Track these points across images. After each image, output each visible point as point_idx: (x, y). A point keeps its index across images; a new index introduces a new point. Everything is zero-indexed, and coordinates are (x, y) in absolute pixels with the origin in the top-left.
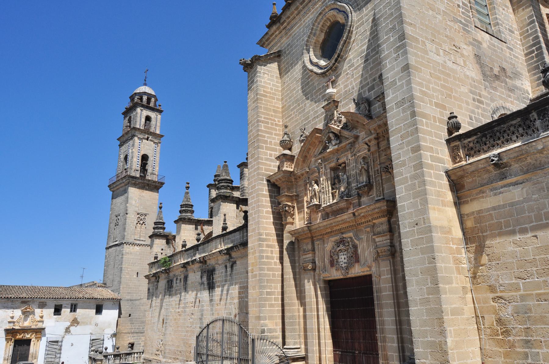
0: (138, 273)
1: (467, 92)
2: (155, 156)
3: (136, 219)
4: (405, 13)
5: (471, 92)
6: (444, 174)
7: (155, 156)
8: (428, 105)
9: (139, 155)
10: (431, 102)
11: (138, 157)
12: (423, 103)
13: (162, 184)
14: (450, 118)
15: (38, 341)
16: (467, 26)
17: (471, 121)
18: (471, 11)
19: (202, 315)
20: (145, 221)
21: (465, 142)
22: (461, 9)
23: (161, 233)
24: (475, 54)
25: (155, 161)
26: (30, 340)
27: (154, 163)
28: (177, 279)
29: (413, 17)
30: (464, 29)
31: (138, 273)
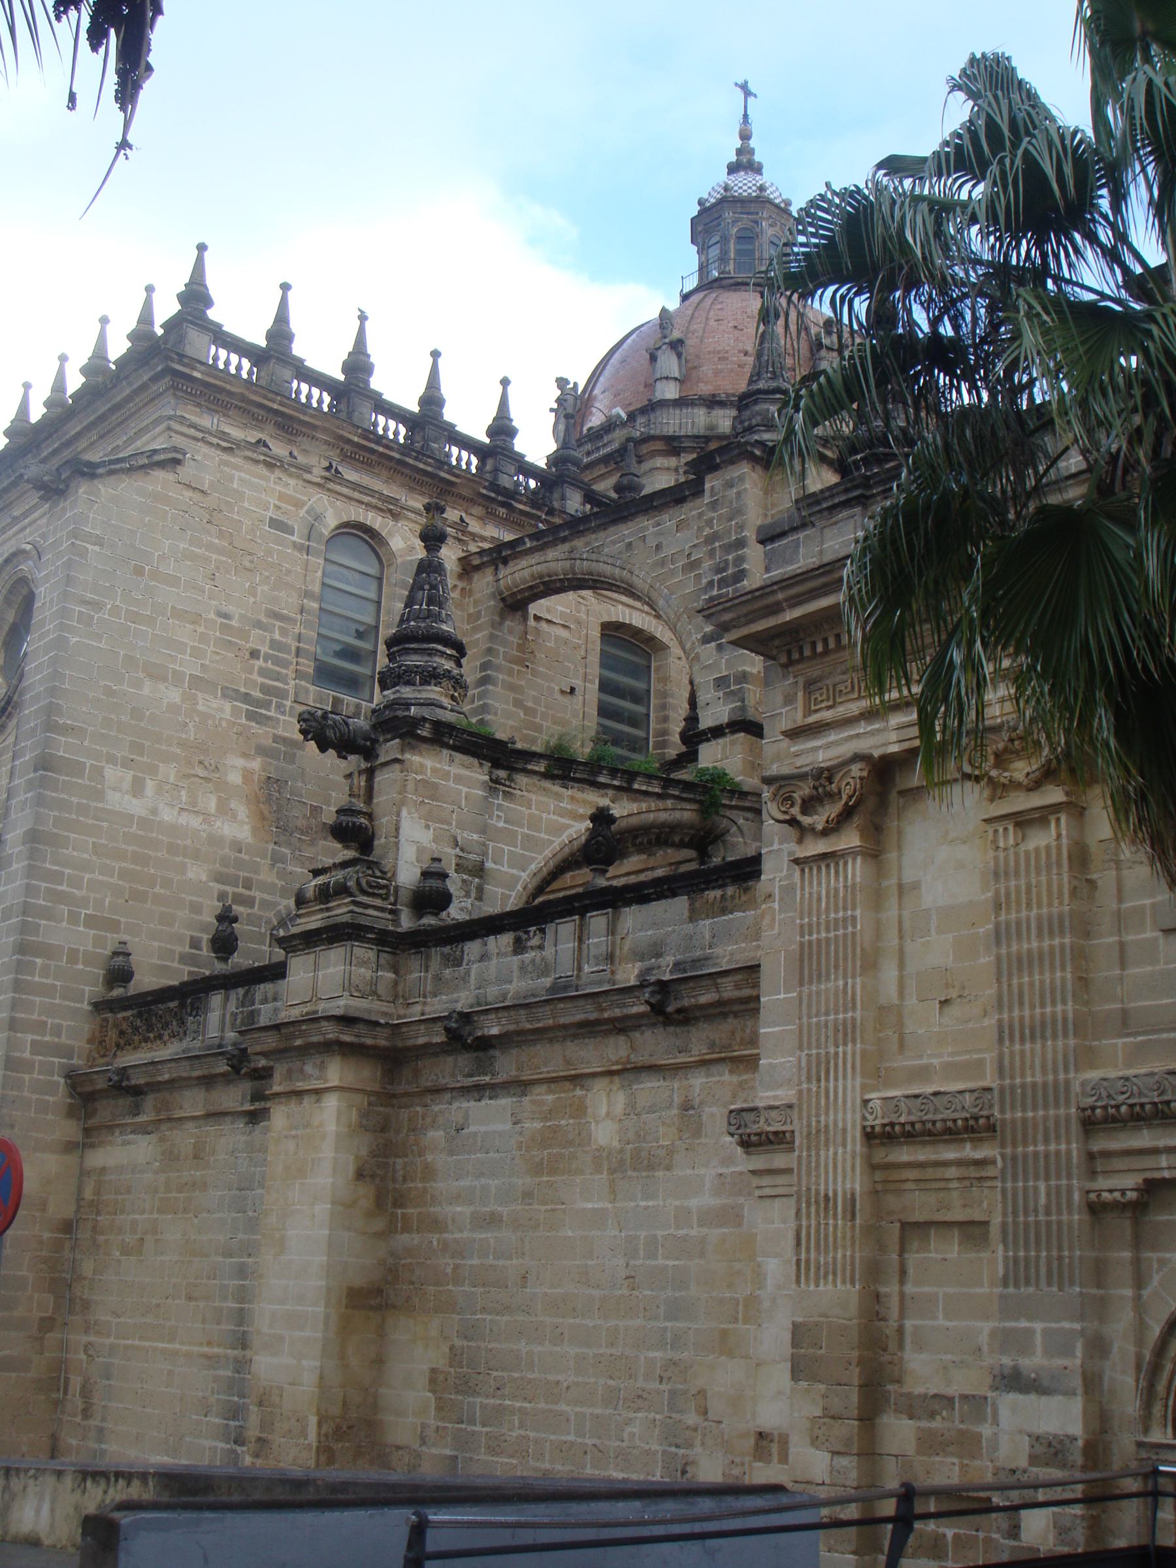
1: (204, 878)
4: (60, 702)
5: (219, 878)
6: (62, 1081)
8: (64, 924)
10: (73, 918)
12: (49, 920)
14: (116, 954)
16: (267, 705)
17: (194, 951)
18: (294, 660)
21: (120, 1015)
22: (260, 663)
24: (269, 778)
29: (84, 709)
30: (251, 716)
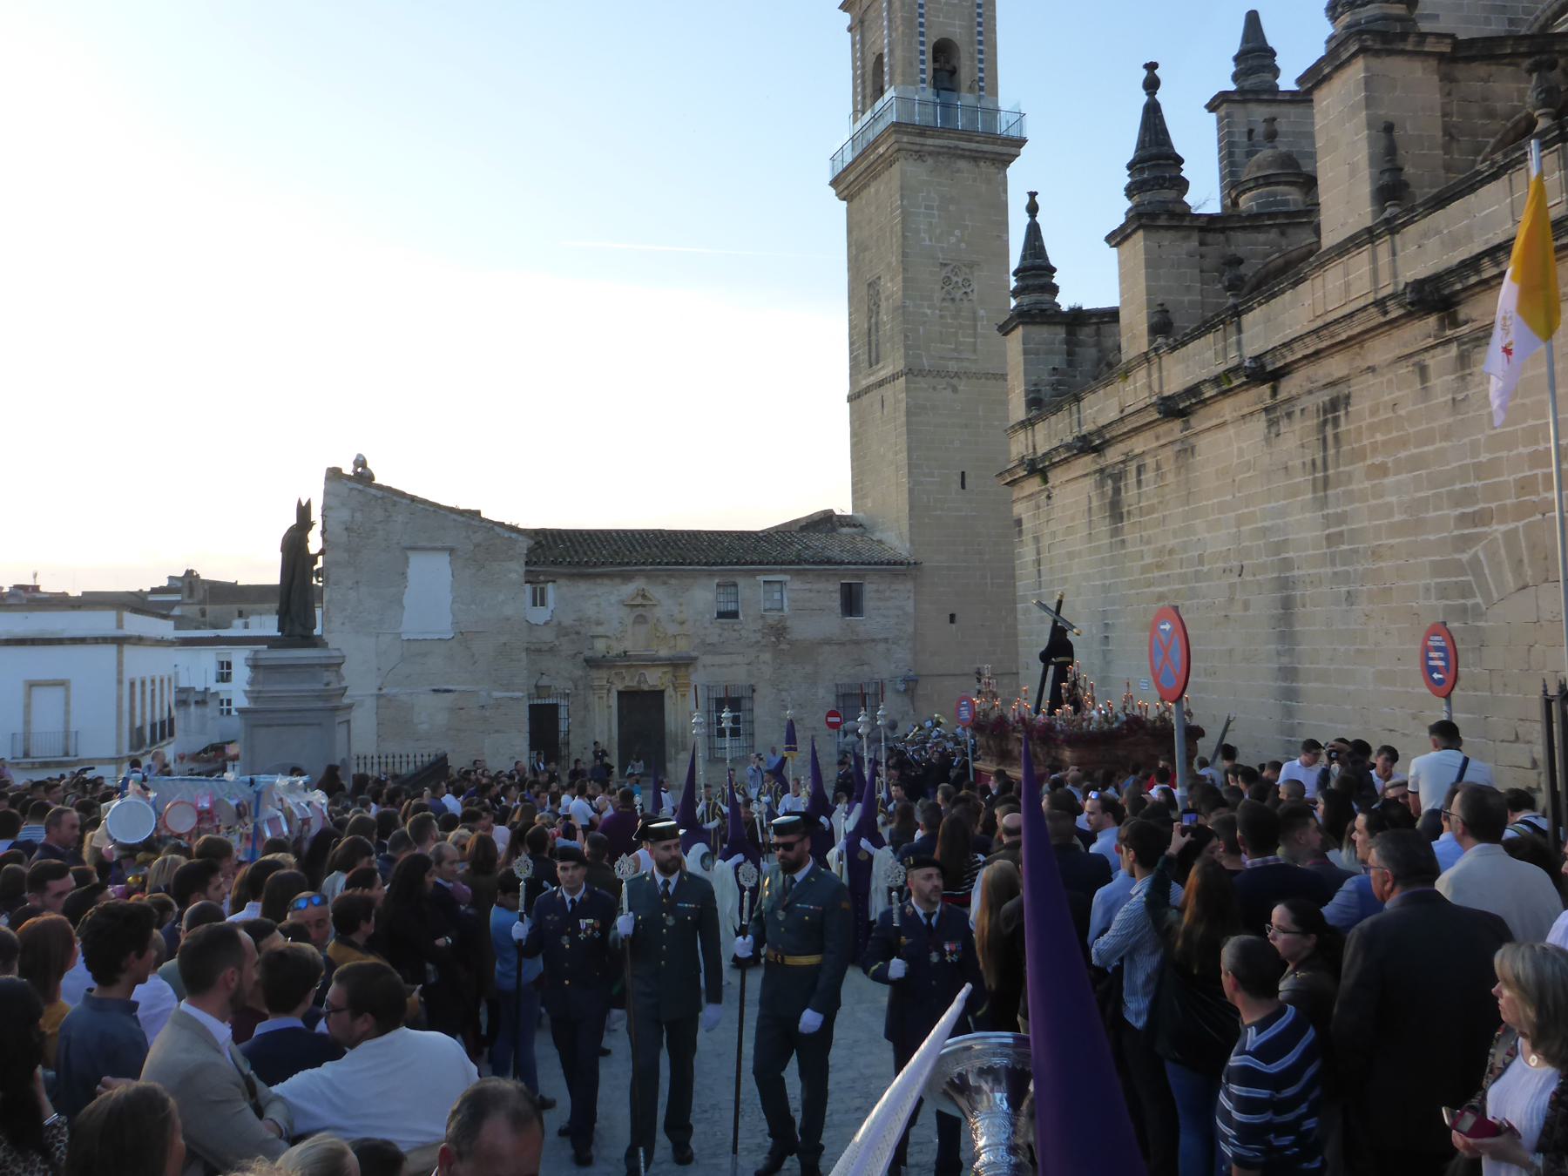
0: (963, 473)
2: (980, 43)
3: (938, 287)
7: (980, 43)
9: (922, 43)
11: (922, 53)
13: (1021, 142)
15: (683, 696)
19: (1287, 604)
20: (969, 290)
23: (1044, 307)
25: (981, 61)
26: (662, 692)
27: (981, 70)
28: (1139, 470)
31: (963, 473)
